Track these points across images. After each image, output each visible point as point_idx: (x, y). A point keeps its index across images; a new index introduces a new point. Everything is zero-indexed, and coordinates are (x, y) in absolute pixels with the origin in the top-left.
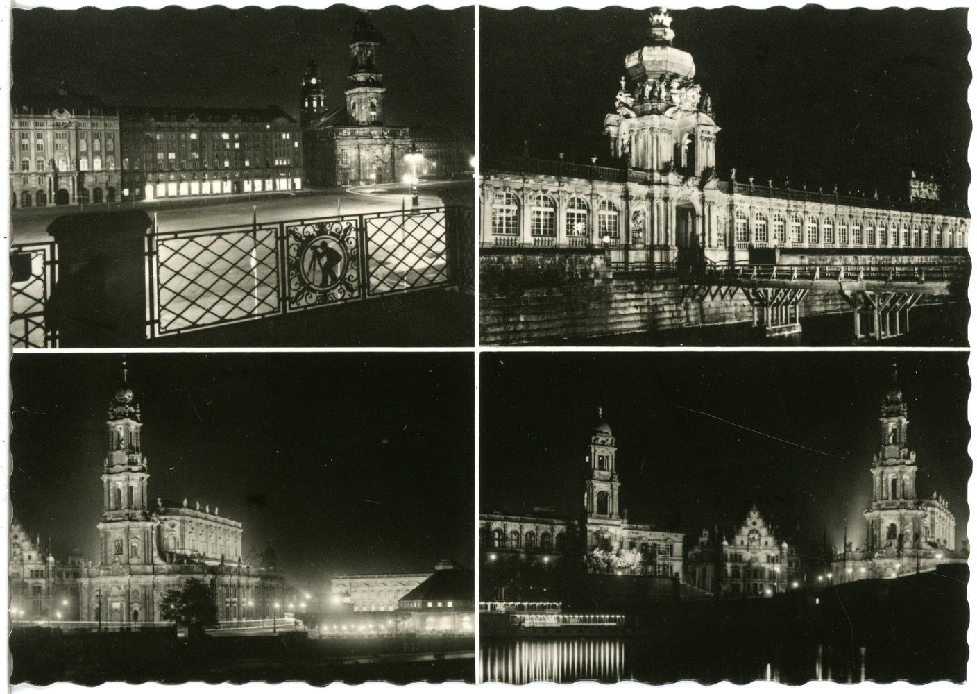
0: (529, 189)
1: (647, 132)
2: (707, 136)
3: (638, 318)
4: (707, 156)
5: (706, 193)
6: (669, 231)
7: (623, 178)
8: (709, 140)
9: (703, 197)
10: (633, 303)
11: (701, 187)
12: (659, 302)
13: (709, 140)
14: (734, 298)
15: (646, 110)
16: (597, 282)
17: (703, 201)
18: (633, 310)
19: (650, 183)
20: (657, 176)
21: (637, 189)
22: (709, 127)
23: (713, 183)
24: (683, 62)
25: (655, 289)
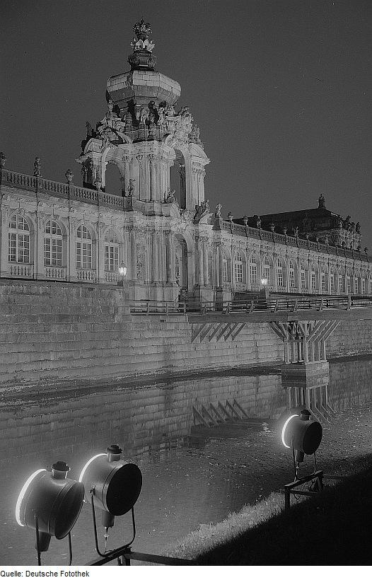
0: (42, 213)
1: (145, 160)
2: (198, 168)
3: (157, 359)
4: (197, 190)
5: (201, 228)
6: (170, 266)
7: (129, 208)
8: (199, 172)
9: (197, 232)
10: (150, 343)
11: (196, 222)
12: (174, 342)
13: (199, 172)
14: (236, 339)
15: (142, 136)
16: (117, 319)
17: (197, 238)
18: (154, 351)
19: (152, 214)
20: (157, 207)
21: (140, 220)
22: (197, 158)
23: (206, 218)
24: (169, 87)
25: (169, 327)
